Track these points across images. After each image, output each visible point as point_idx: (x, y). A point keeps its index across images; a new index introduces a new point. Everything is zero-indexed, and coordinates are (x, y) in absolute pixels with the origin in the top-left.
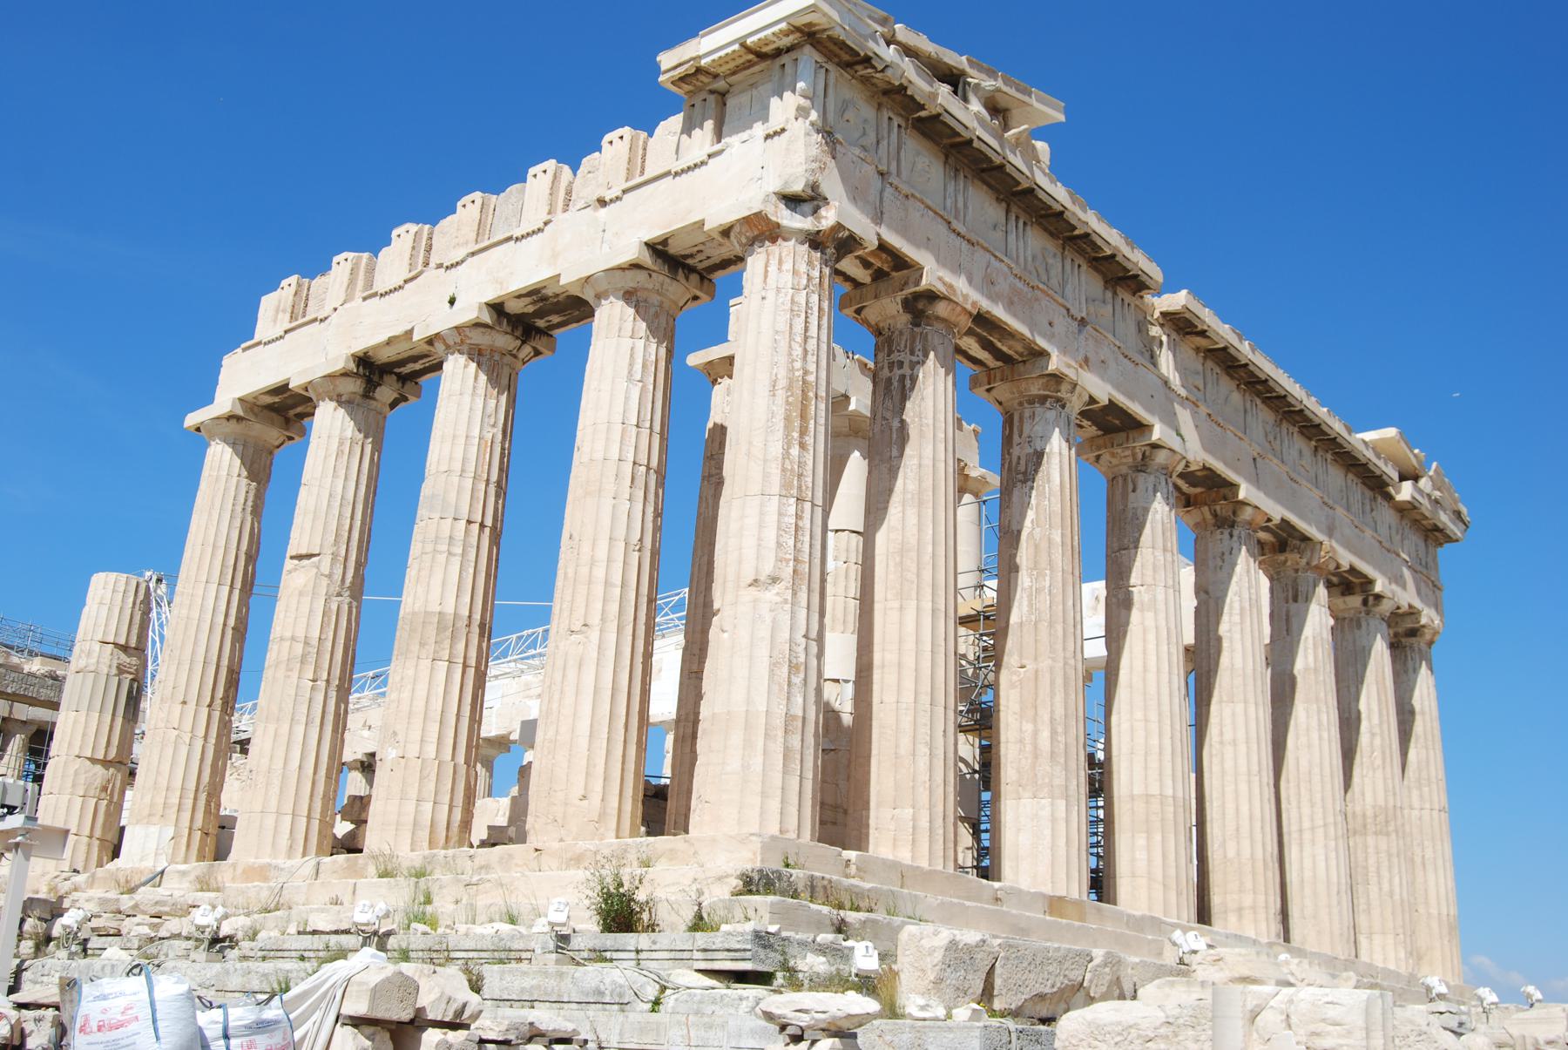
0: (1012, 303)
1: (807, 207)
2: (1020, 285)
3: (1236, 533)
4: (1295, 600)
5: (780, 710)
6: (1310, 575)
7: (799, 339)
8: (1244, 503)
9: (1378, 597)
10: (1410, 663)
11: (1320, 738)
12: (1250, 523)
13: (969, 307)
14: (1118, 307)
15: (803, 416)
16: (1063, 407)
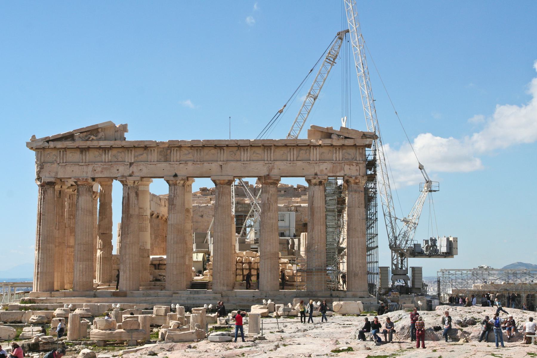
6: (264, 185)
9: (310, 180)
12: (220, 184)
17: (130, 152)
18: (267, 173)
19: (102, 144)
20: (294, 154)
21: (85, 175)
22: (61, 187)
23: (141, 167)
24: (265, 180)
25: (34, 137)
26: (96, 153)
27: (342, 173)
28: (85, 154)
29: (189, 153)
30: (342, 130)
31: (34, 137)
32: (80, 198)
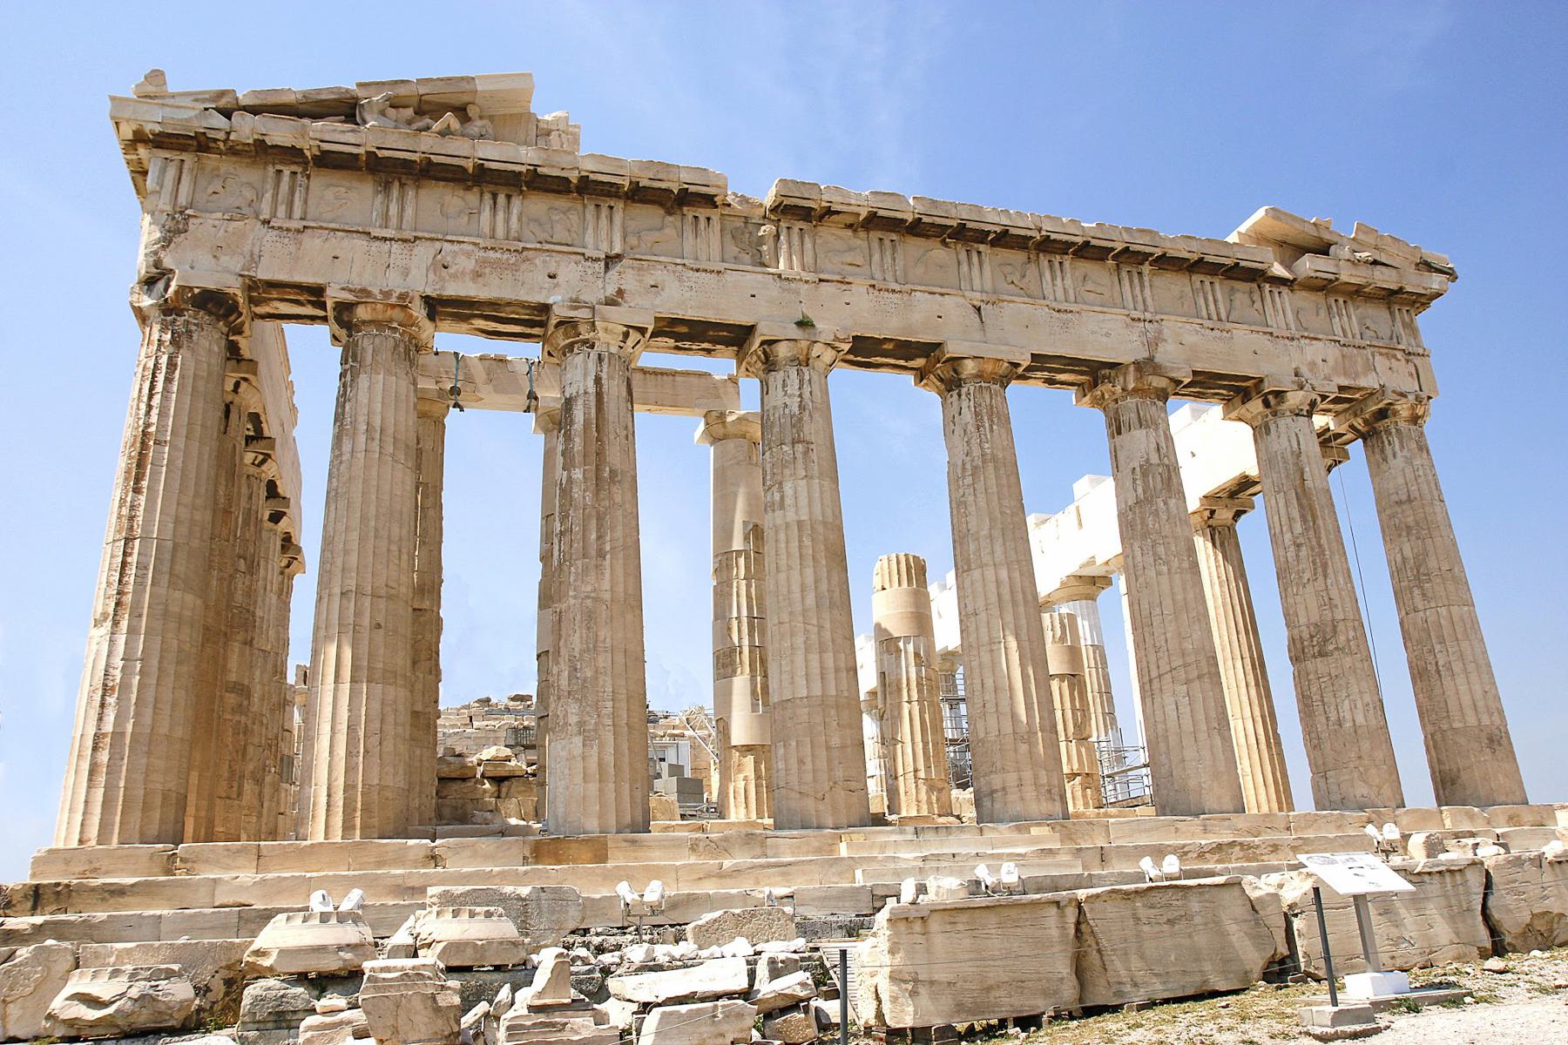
0: (477, 275)
1: (161, 285)
2: (498, 255)
3: (964, 390)
4: (1119, 433)
5: (91, 731)
6: (1131, 401)
7: (145, 399)
8: (956, 361)
9: (1279, 395)
10: (1388, 449)
11: (1159, 573)
12: (980, 376)
13: (393, 300)
14: (688, 229)
15: (140, 465)
16: (592, 347)
17: (604, 212)
18: (1146, 355)
19: (492, 152)
20: (1215, 301)
21: (395, 283)
22: (237, 385)
23: (658, 275)
24: (1139, 379)
25: (156, 76)
26: (454, 199)
27: (1369, 381)
28: (402, 197)
29: (850, 249)
30: (1361, 237)
31: (156, 76)
32: (363, 381)
